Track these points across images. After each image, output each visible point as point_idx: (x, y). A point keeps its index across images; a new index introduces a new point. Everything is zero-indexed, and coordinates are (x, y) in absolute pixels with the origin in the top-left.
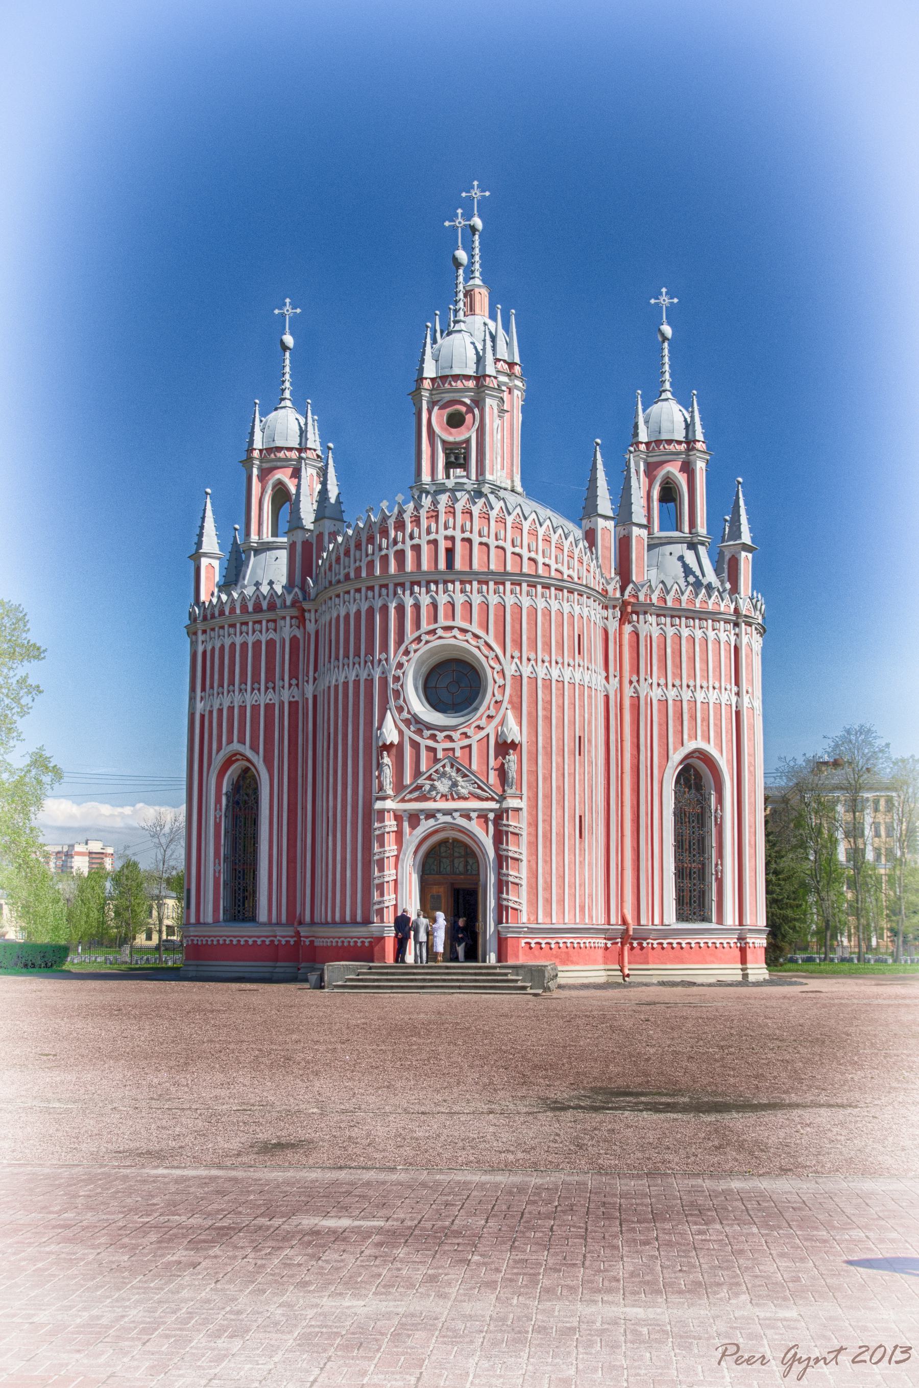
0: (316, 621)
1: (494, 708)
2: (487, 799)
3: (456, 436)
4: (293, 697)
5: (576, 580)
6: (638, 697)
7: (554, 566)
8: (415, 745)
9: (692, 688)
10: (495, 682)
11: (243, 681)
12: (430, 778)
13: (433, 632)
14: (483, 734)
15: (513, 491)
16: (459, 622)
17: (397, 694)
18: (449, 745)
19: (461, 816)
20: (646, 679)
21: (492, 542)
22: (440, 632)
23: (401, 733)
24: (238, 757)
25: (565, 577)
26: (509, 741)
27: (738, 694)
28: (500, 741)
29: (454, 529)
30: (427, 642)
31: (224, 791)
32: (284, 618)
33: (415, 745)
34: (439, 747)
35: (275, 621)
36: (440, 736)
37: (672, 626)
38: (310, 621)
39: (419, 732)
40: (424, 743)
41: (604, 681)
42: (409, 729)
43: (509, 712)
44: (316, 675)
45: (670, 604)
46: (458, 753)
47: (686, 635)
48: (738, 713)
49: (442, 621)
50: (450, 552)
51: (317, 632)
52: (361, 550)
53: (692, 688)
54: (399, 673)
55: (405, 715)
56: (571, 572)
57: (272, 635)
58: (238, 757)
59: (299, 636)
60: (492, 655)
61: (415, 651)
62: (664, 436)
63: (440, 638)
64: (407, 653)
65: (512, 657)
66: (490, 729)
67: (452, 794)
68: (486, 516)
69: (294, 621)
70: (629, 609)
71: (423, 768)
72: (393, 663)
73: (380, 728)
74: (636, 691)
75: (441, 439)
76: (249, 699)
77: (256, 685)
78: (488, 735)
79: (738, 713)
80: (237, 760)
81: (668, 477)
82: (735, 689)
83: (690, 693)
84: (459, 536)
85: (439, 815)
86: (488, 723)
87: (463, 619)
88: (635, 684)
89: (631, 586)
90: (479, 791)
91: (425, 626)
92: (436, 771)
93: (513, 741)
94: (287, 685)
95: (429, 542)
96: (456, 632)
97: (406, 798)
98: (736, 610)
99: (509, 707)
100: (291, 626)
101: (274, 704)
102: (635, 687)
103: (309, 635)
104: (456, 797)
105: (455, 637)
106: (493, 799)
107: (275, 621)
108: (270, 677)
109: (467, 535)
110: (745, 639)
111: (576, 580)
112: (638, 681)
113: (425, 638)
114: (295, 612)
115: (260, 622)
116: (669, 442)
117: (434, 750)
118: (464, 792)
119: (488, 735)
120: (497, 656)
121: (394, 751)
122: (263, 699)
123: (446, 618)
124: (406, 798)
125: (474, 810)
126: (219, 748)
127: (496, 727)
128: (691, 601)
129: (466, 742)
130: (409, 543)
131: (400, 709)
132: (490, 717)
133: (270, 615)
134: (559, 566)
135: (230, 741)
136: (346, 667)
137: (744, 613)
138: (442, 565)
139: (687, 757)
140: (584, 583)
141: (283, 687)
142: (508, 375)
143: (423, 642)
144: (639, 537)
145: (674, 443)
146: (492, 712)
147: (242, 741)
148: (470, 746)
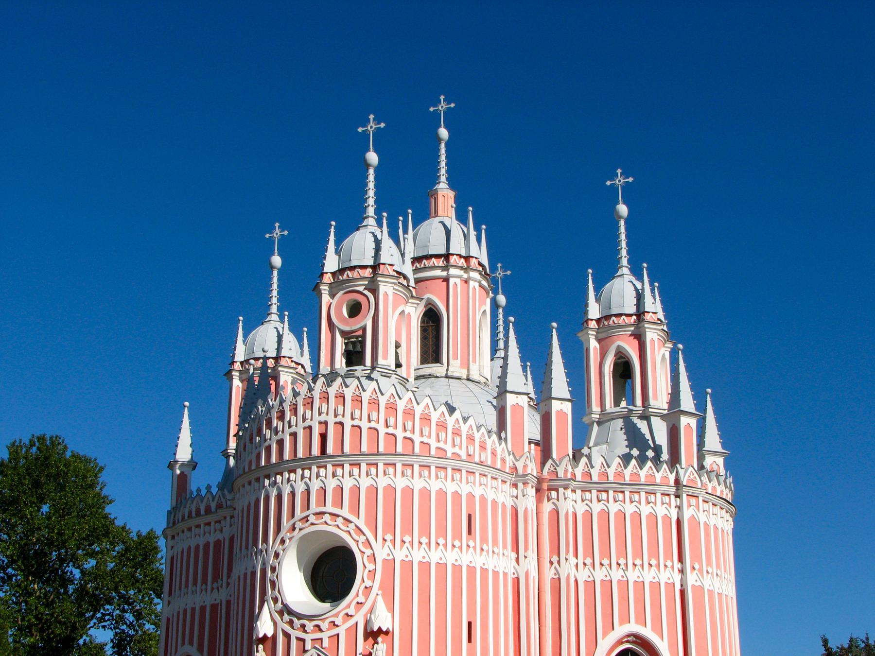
1: (364, 594)
3: (353, 325)
5: (464, 457)
6: (559, 579)
7: (434, 444)
8: (287, 635)
9: (622, 566)
10: (365, 567)
11: (195, 583)
14: (351, 622)
15: (468, 379)
16: (329, 508)
17: (273, 584)
18: (318, 635)
20: (567, 559)
21: (365, 425)
22: (312, 519)
23: (275, 624)
25: (449, 455)
26: (375, 629)
27: (682, 571)
32: (225, 518)
33: (287, 635)
34: (308, 638)
36: (310, 626)
37: (599, 501)
39: (291, 623)
40: (295, 634)
41: (514, 563)
43: (380, 598)
45: (595, 478)
46: (326, 643)
47: (616, 510)
48: (683, 593)
50: (323, 437)
53: (622, 566)
56: (457, 450)
57: (219, 536)
62: (615, 311)
63: (312, 524)
65: (385, 540)
66: (360, 619)
68: (359, 399)
70: (545, 486)
74: (557, 573)
75: (338, 328)
79: (683, 593)
81: (620, 352)
82: (677, 566)
83: (621, 572)
84: (331, 420)
87: (334, 505)
88: (556, 564)
89: (550, 462)
91: (298, 513)
93: (380, 629)
94: (225, 585)
95: (304, 428)
96: (327, 518)
98: (677, 482)
99: (380, 592)
101: (218, 604)
102: (555, 568)
105: (326, 523)
107: (219, 522)
108: (216, 578)
109: (339, 419)
110: (687, 514)
111: (464, 457)
112: (559, 562)
113: (299, 525)
116: (619, 315)
117: (303, 640)
120: (367, 539)
121: (269, 644)
122: (208, 599)
123: (318, 505)
127: (366, 615)
128: (620, 475)
129: (335, 631)
131: (275, 600)
134: (441, 445)
135: (183, 644)
137: (685, 483)
138: (316, 451)
139: (620, 642)
140: (477, 460)
142: (462, 268)
143: (297, 530)
144: (561, 413)
145: (624, 317)
146: (361, 599)
147: (191, 643)
148: (338, 635)
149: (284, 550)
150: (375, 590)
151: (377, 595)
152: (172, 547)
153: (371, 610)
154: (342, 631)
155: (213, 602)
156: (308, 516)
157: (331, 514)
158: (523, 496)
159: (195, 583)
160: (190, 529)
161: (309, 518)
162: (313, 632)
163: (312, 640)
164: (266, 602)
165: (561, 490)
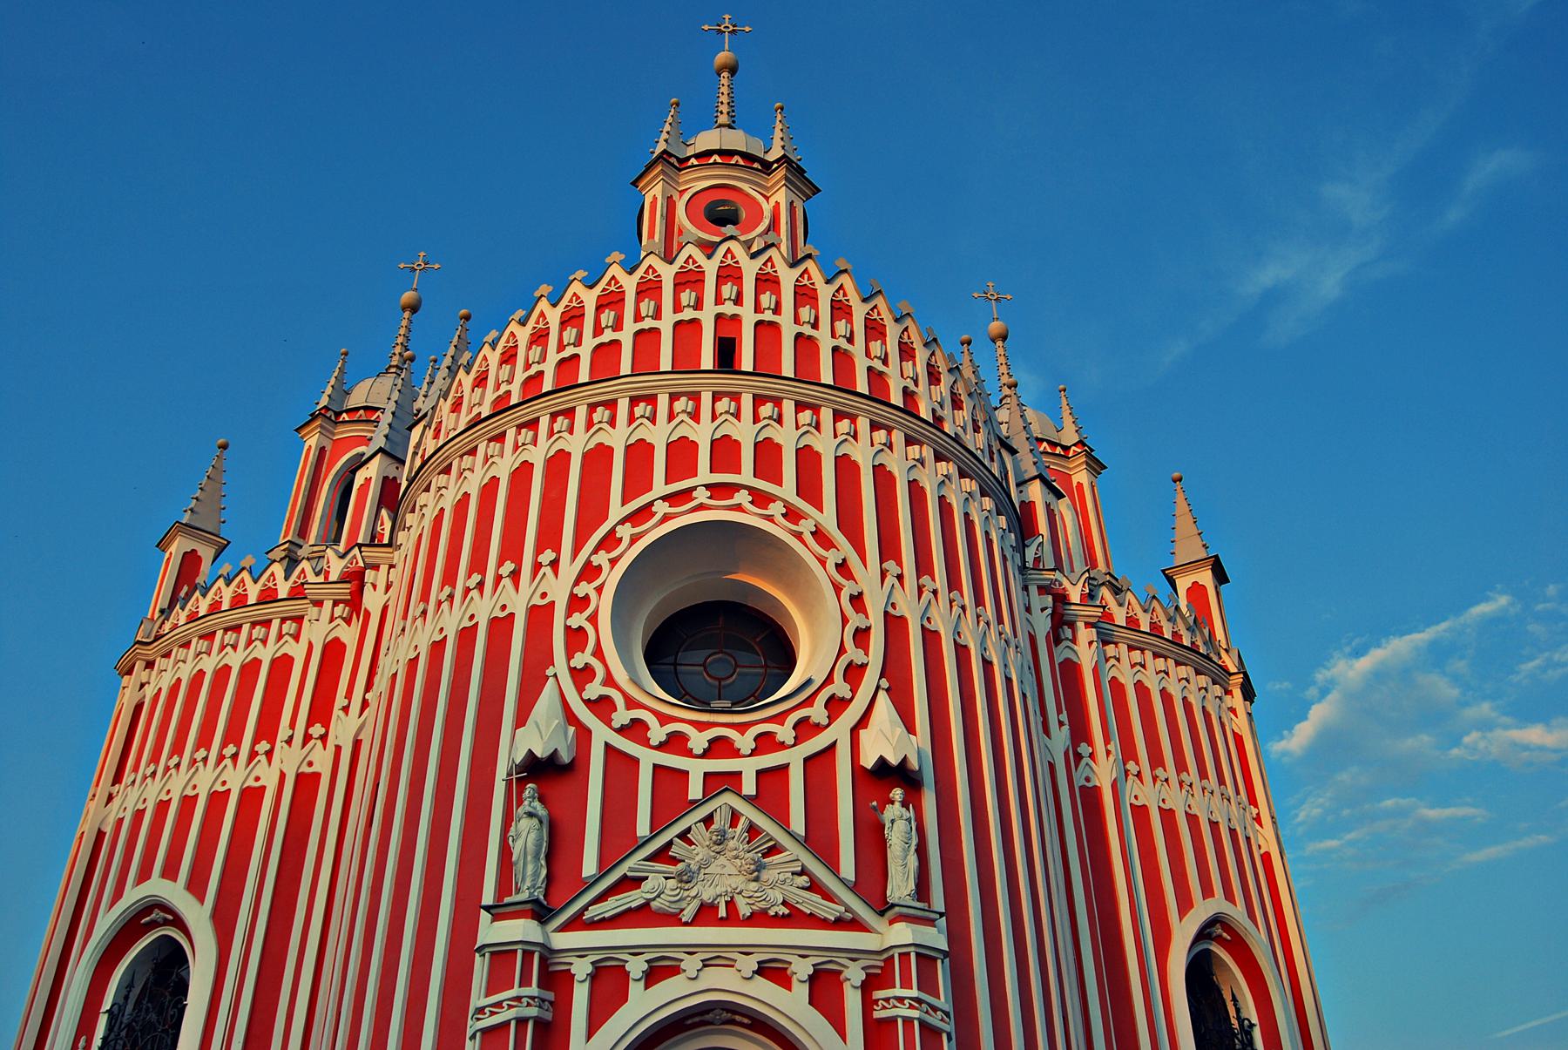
0: (388, 587)
2: (840, 924)
4: (310, 764)
8: (620, 766)
11: (204, 741)
12: (662, 855)
13: (686, 494)
17: (576, 639)
19: (763, 970)
20: (1108, 753)
24: (156, 915)
28: (868, 761)
29: (738, 301)
30: (666, 518)
31: (107, 1005)
33: (620, 766)
34: (697, 769)
35: (299, 620)
38: (374, 587)
40: (648, 758)
42: (608, 722)
43: (882, 695)
44: (368, 696)
49: (704, 475)
51: (385, 609)
52: (514, 364)
54: (584, 589)
55: (594, 690)
58: (156, 915)
59: (344, 639)
60: (833, 557)
61: (634, 539)
64: (610, 541)
67: (731, 905)
69: (339, 610)
71: (643, 829)
72: (569, 570)
73: (521, 721)
76: (204, 782)
77: (231, 749)
78: (833, 746)
80: (154, 925)
82: (1255, 811)
84: (749, 318)
85: (691, 964)
86: (832, 719)
90: (817, 898)
91: (660, 487)
92: (683, 836)
96: (742, 497)
97: (587, 915)
99: (885, 683)
100: (332, 619)
101: (263, 788)
103: (368, 614)
104: (744, 910)
106: (855, 924)
114: (345, 590)
115: (267, 623)
118: (774, 900)
119: (833, 746)
122: (236, 780)
124: (587, 915)
125: (804, 951)
126: (118, 893)
127: (855, 731)
130: (630, 328)
131: (582, 676)
132: (836, 706)
133: (294, 607)
135: (144, 875)
136: (445, 606)
141: (289, 742)
146: (840, 688)
147: (170, 872)
148: (784, 768)
149: (613, 562)
150: (871, 678)
151: (878, 687)
152: (142, 685)
153: (863, 721)
154: (794, 758)
155: (251, 783)
156: (695, 488)
157: (752, 491)
158: (1043, 610)
159: (204, 741)
160: (210, 636)
161: (695, 494)
162: (706, 754)
163: (708, 776)
164: (551, 680)
165: (1080, 625)
